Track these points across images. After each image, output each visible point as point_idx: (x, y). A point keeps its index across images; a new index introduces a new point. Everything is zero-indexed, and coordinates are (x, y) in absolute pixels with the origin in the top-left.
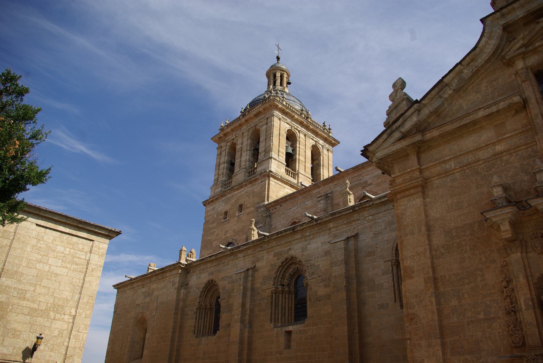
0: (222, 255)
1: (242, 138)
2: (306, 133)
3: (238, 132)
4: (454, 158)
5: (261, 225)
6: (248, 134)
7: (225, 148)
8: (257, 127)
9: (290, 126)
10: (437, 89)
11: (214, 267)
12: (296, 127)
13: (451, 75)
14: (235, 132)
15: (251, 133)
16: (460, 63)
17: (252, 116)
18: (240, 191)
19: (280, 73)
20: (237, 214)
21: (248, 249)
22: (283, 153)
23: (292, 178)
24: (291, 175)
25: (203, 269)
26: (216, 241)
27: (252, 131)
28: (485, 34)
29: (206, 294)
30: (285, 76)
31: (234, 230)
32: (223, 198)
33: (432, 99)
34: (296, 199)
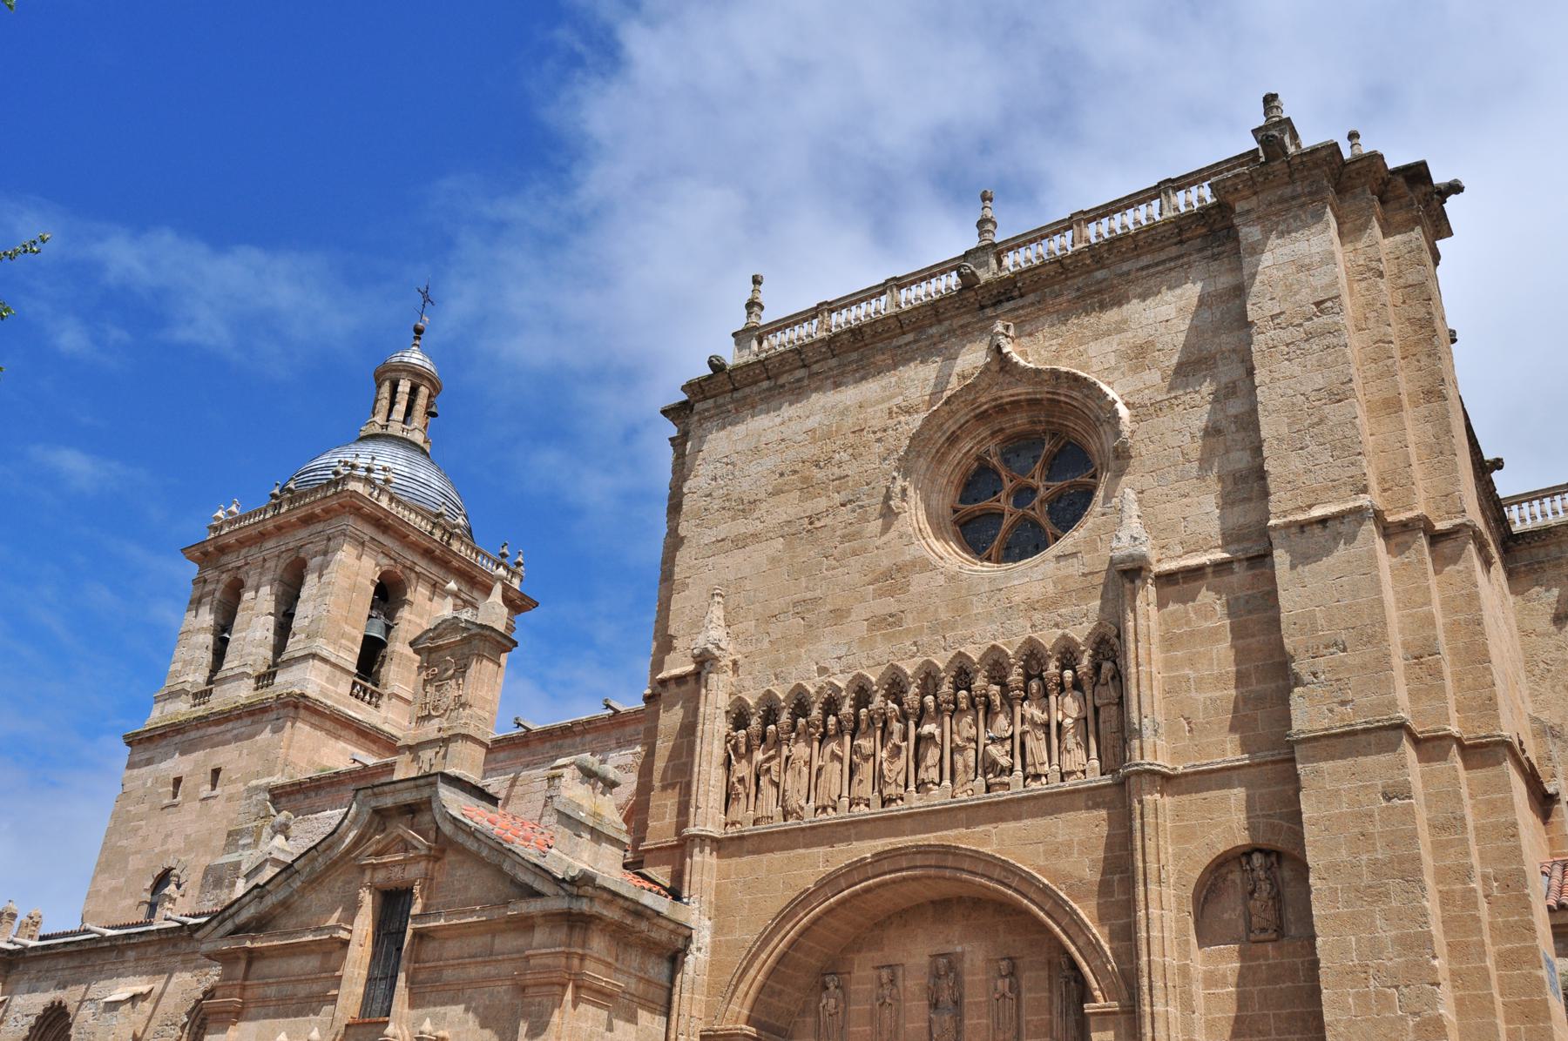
0: (94, 946)
1: (261, 574)
2: (435, 578)
3: (254, 550)
4: (276, 982)
5: (249, 840)
6: (276, 566)
7: (213, 586)
8: (302, 555)
9: (392, 562)
10: (284, 875)
11: (73, 971)
12: (408, 564)
13: (303, 860)
14: (246, 550)
15: (284, 566)
16: (315, 847)
17: (293, 519)
18: (222, 728)
19: (409, 384)
20: (206, 790)
21: (150, 943)
22: (353, 640)
23: (370, 708)
24: (367, 697)
25: (47, 971)
26: (139, 856)
27: (288, 561)
28: (349, 816)
29: (43, 1033)
30: (424, 391)
31: (187, 836)
32: (178, 738)
33: (279, 886)
34: (342, 788)
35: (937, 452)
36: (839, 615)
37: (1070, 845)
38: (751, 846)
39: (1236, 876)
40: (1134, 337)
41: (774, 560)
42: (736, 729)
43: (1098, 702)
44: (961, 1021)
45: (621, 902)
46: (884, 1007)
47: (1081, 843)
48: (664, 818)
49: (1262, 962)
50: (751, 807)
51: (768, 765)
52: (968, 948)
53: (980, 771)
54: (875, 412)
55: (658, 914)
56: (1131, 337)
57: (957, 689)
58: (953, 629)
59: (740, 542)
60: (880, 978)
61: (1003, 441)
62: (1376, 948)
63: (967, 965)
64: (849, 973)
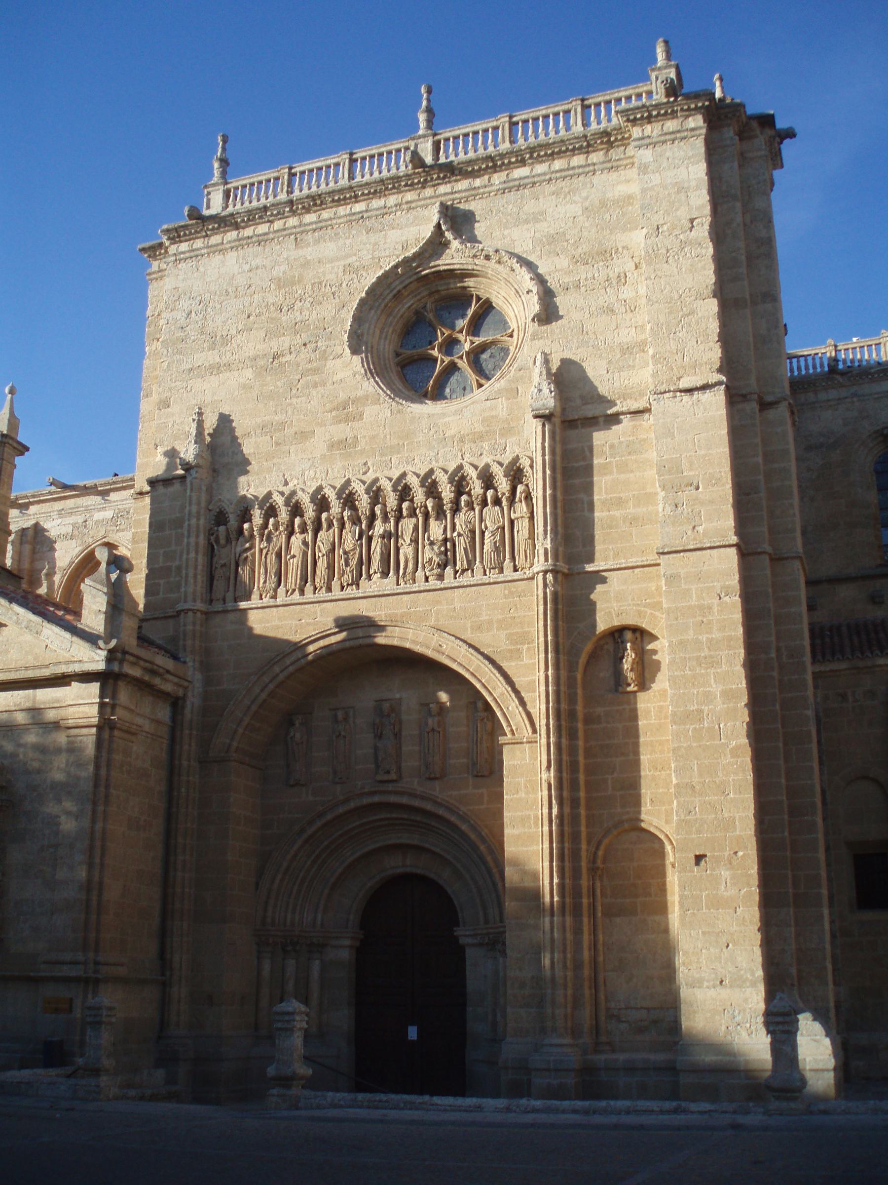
35: (386, 306)
36: (303, 436)
37: (490, 622)
40: (549, 227)
41: (246, 387)
43: (513, 517)
44: (400, 748)
45: (142, 663)
47: (499, 621)
48: (158, 594)
50: (231, 588)
51: (245, 555)
53: (420, 565)
54: (333, 268)
55: (168, 672)
56: (544, 228)
58: (398, 453)
59: (216, 369)
60: (336, 716)
61: (436, 301)
62: (708, 698)
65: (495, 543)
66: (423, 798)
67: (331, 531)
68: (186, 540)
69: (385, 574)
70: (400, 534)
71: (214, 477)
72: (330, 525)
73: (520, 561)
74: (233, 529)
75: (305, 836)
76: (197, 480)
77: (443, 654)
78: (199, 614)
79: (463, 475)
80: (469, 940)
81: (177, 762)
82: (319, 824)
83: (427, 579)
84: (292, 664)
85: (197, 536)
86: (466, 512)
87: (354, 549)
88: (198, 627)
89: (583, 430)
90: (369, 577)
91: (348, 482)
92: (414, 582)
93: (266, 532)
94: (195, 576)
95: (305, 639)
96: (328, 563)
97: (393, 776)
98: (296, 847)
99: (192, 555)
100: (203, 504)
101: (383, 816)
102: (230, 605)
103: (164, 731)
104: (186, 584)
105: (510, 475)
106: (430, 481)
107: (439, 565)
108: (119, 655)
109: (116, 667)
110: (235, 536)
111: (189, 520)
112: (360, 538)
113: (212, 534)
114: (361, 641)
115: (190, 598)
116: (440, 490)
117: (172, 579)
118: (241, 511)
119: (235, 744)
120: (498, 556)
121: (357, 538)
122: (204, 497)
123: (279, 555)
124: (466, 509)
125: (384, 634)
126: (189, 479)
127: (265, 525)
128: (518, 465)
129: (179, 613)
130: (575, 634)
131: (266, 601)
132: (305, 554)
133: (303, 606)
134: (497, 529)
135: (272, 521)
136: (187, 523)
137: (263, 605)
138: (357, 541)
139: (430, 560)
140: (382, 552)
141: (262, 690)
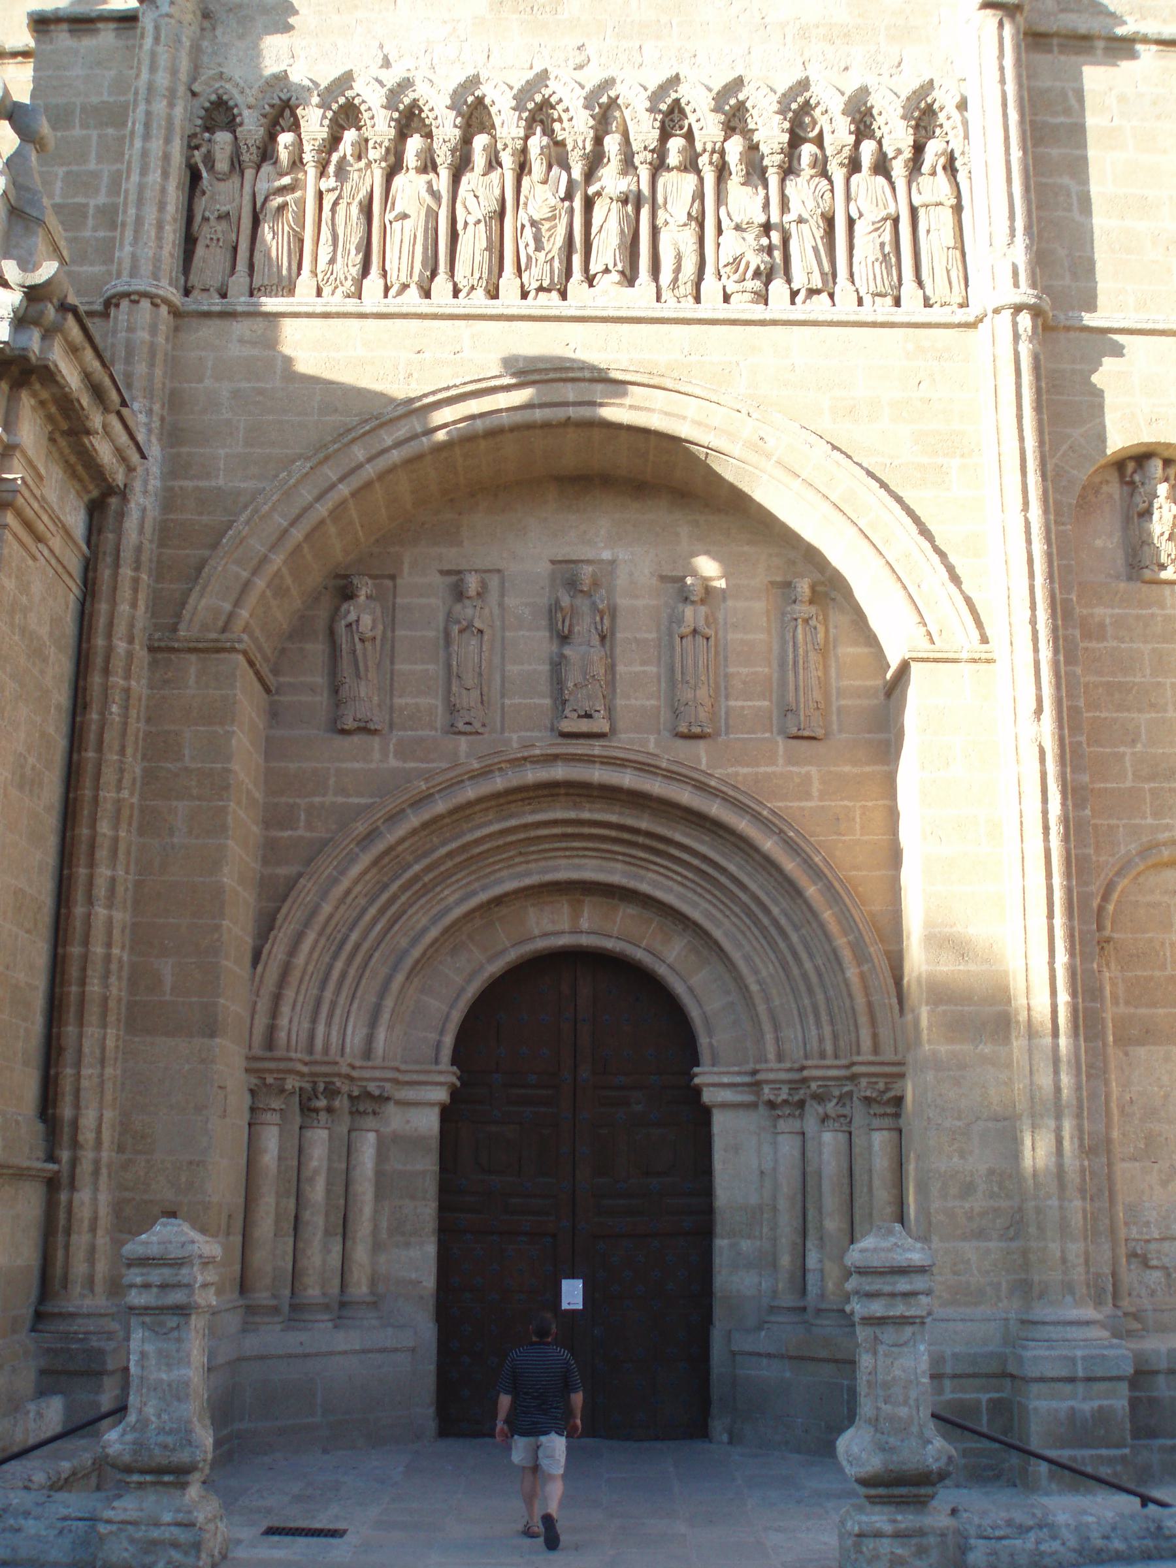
38: (248, 333)
39: (1114, 488)
42: (209, 129)
45: (89, 354)
46: (466, 635)
49: (1155, 610)
50: (241, 265)
52: (623, 554)
53: (710, 269)
57: (665, 136)
63: (622, 580)
64: (393, 577)
65: (882, 245)
66: (671, 776)
67: (495, 176)
68: (138, 144)
69: (630, 278)
70: (660, 200)
71: (203, 29)
72: (494, 163)
73: (937, 287)
74: (250, 142)
75: (380, 846)
76: (173, 21)
77: (768, 456)
78: (164, 309)
79: (807, 103)
80: (727, 1096)
81: (100, 642)
82: (414, 820)
83: (727, 298)
84: (398, 444)
85: (168, 141)
86: (812, 177)
87: (553, 218)
88: (161, 340)
89: (1063, 58)
90: (590, 280)
91: (543, 77)
92: (698, 299)
93: (335, 157)
94: (160, 227)
95: (425, 395)
96: (489, 239)
97: (600, 724)
98: (355, 871)
99: (155, 177)
100: (183, 76)
101: (560, 815)
102: (239, 301)
103: (75, 564)
104: (136, 239)
105: (912, 118)
106: (733, 101)
107: (757, 274)
108: (51, 312)
109: (33, 341)
110: (254, 158)
111: (148, 101)
112: (569, 196)
113: (197, 147)
114: (571, 412)
115: (146, 268)
116: (751, 126)
117: (87, 234)
118: (272, 106)
119: (244, 613)
120: (889, 274)
121: (562, 194)
122: (184, 65)
123: (367, 210)
124: (813, 172)
125: (627, 401)
126: (147, 22)
127: (334, 141)
128: (929, 100)
129: (111, 303)
130: (1065, 447)
131: (334, 301)
132: (431, 215)
133: (427, 323)
134: (885, 219)
135: (350, 136)
136: (142, 107)
137: (328, 309)
138: (563, 200)
139: (736, 261)
140: (622, 231)
141: (319, 498)
